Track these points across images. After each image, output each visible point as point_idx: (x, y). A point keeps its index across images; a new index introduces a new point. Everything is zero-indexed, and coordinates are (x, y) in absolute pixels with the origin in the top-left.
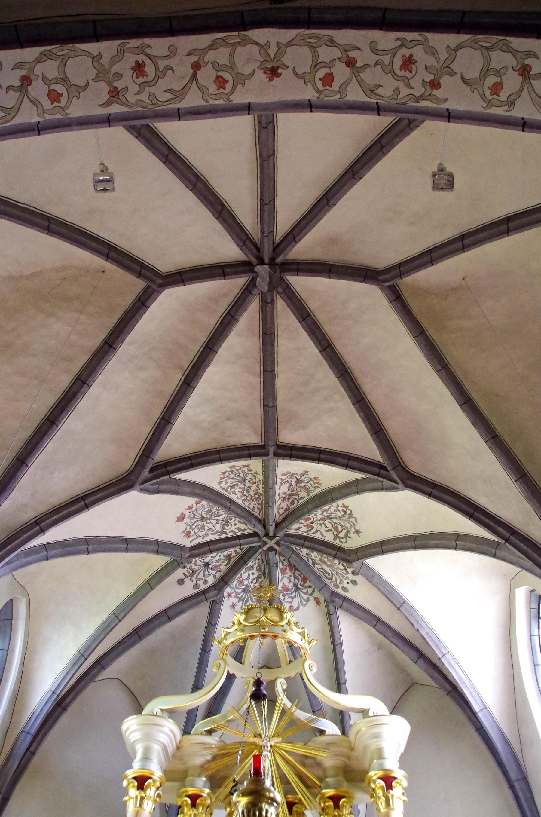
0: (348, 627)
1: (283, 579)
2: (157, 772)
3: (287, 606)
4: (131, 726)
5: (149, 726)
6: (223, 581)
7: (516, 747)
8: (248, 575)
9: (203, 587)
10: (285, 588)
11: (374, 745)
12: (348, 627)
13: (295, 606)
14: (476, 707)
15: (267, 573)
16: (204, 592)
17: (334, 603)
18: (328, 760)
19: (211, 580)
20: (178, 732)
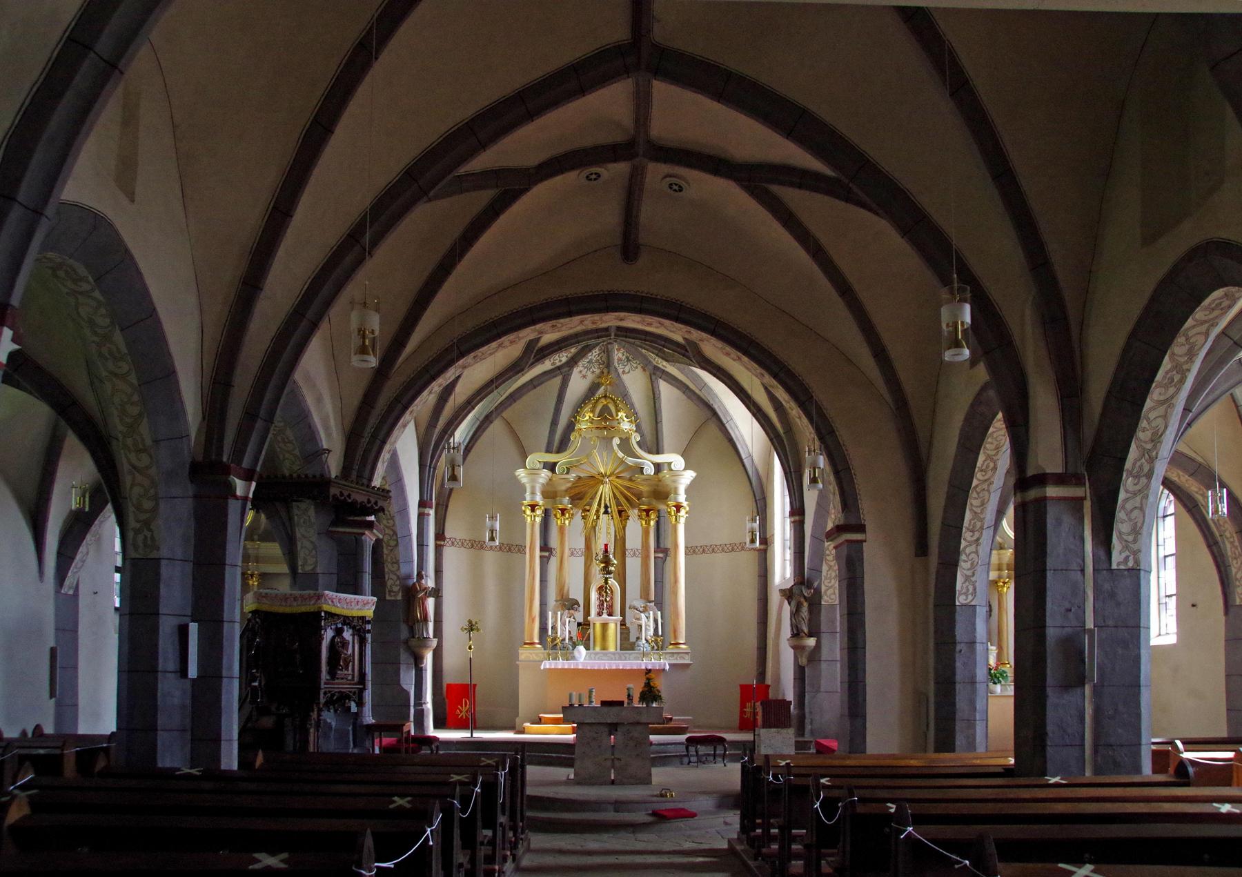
0: (664, 387)
1: (618, 354)
2: (539, 499)
3: (620, 371)
4: (521, 474)
5: (533, 473)
6: (573, 362)
7: (764, 480)
8: (594, 355)
9: (558, 364)
10: (619, 360)
11: (672, 485)
12: (664, 387)
13: (627, 369)
14: (743, 456)
15: (607, 353)
16: (559, 368)
17: (655, 374)
18: (644, 489)
19: (564, 360)
20: (549, 474)
